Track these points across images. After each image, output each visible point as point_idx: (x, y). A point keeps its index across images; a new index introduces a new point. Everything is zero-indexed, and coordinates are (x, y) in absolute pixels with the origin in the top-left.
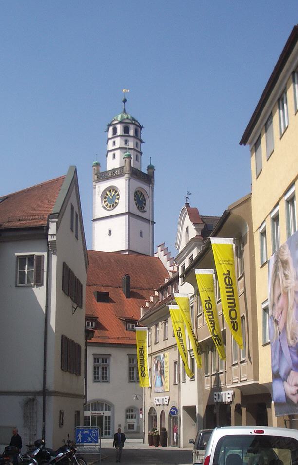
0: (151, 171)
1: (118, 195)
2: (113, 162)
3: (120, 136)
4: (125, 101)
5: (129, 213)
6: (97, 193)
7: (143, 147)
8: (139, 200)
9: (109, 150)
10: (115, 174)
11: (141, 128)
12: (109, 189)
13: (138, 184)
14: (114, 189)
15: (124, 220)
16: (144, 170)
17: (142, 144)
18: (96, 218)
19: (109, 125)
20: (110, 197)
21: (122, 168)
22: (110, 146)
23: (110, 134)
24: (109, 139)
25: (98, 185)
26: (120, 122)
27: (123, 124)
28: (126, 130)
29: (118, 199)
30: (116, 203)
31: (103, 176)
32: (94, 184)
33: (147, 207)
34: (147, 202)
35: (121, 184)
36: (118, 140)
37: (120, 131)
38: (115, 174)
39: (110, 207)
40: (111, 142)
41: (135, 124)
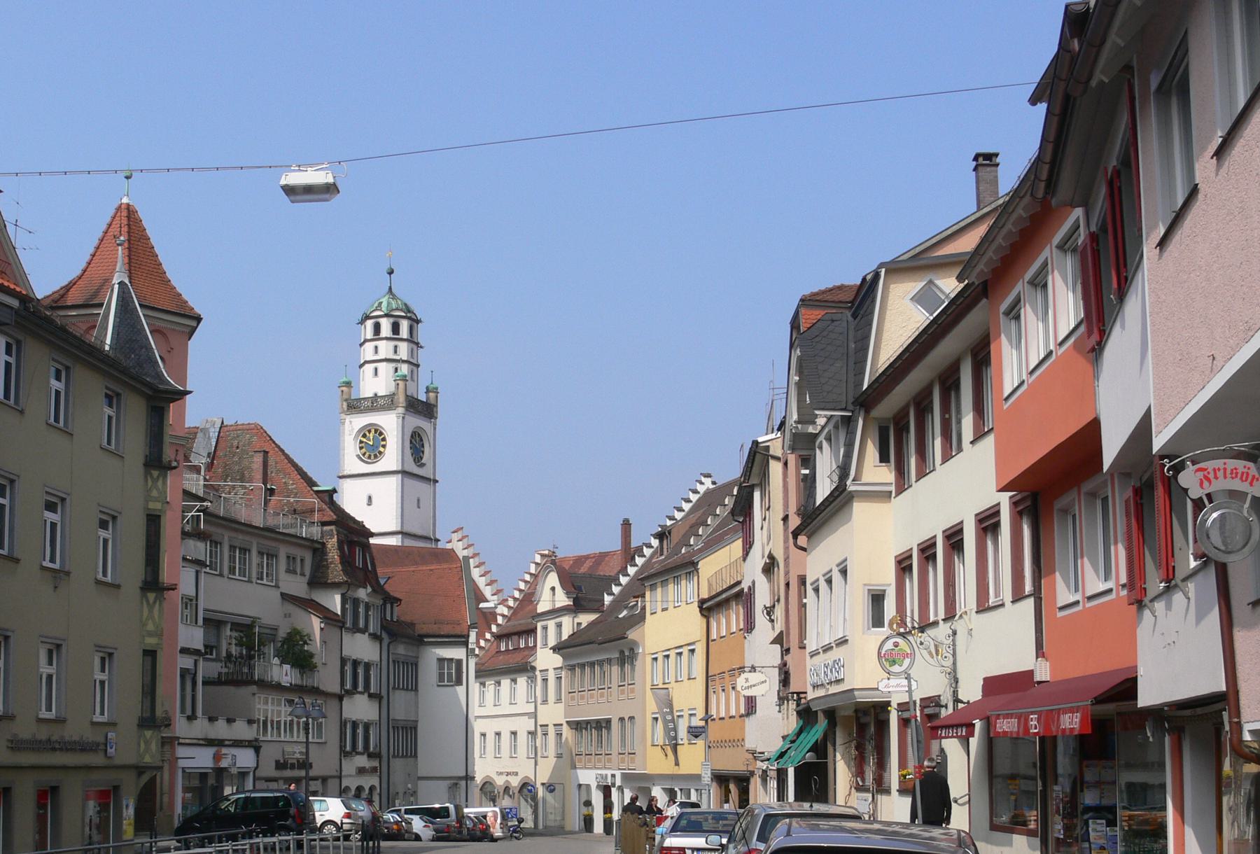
0: (432, 395)
1: (384, 439)
2: (376, 382)
3: (387, 339)
4: (391, 272)
5: (404, 473)
6: (347, 432)
7: (422, 356)
8: (416, 444)
9: (368, 359)
10: (376, 404)
11: (418, 322)
12: (366, 431)
13: (416, 422)
14: (379, 432)
15: (394, 481)
16: (422, 397)
17: (420, 350)
18: (345, 473)
19: (368, 317)
20: (372, 444)
21: (392, 396)
22: (368, 352)
23: (369, 335)
24: (366, 341)
25: (348, 419)
26: (387, 315)
27: (392, 320)
28: (396, 328)
29: (384, 446)
30: (380, 453)
31: (354, 406)
32: (343, 416)
33: (426, 458)
34: (427, 449)
35: (390, 422)
36: (382, 345)
37: (386, 330)
38: (376, 404)
39: (369, 457)
40: (369, 347)
41: (409, 318)
